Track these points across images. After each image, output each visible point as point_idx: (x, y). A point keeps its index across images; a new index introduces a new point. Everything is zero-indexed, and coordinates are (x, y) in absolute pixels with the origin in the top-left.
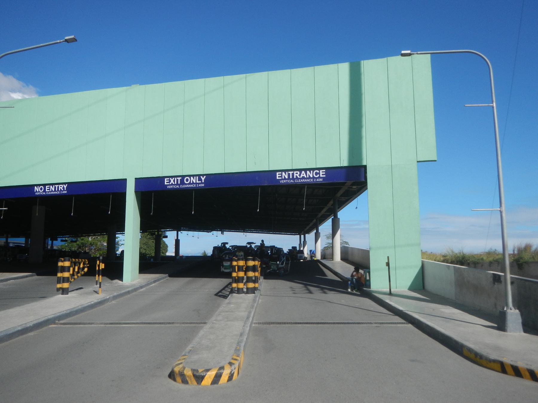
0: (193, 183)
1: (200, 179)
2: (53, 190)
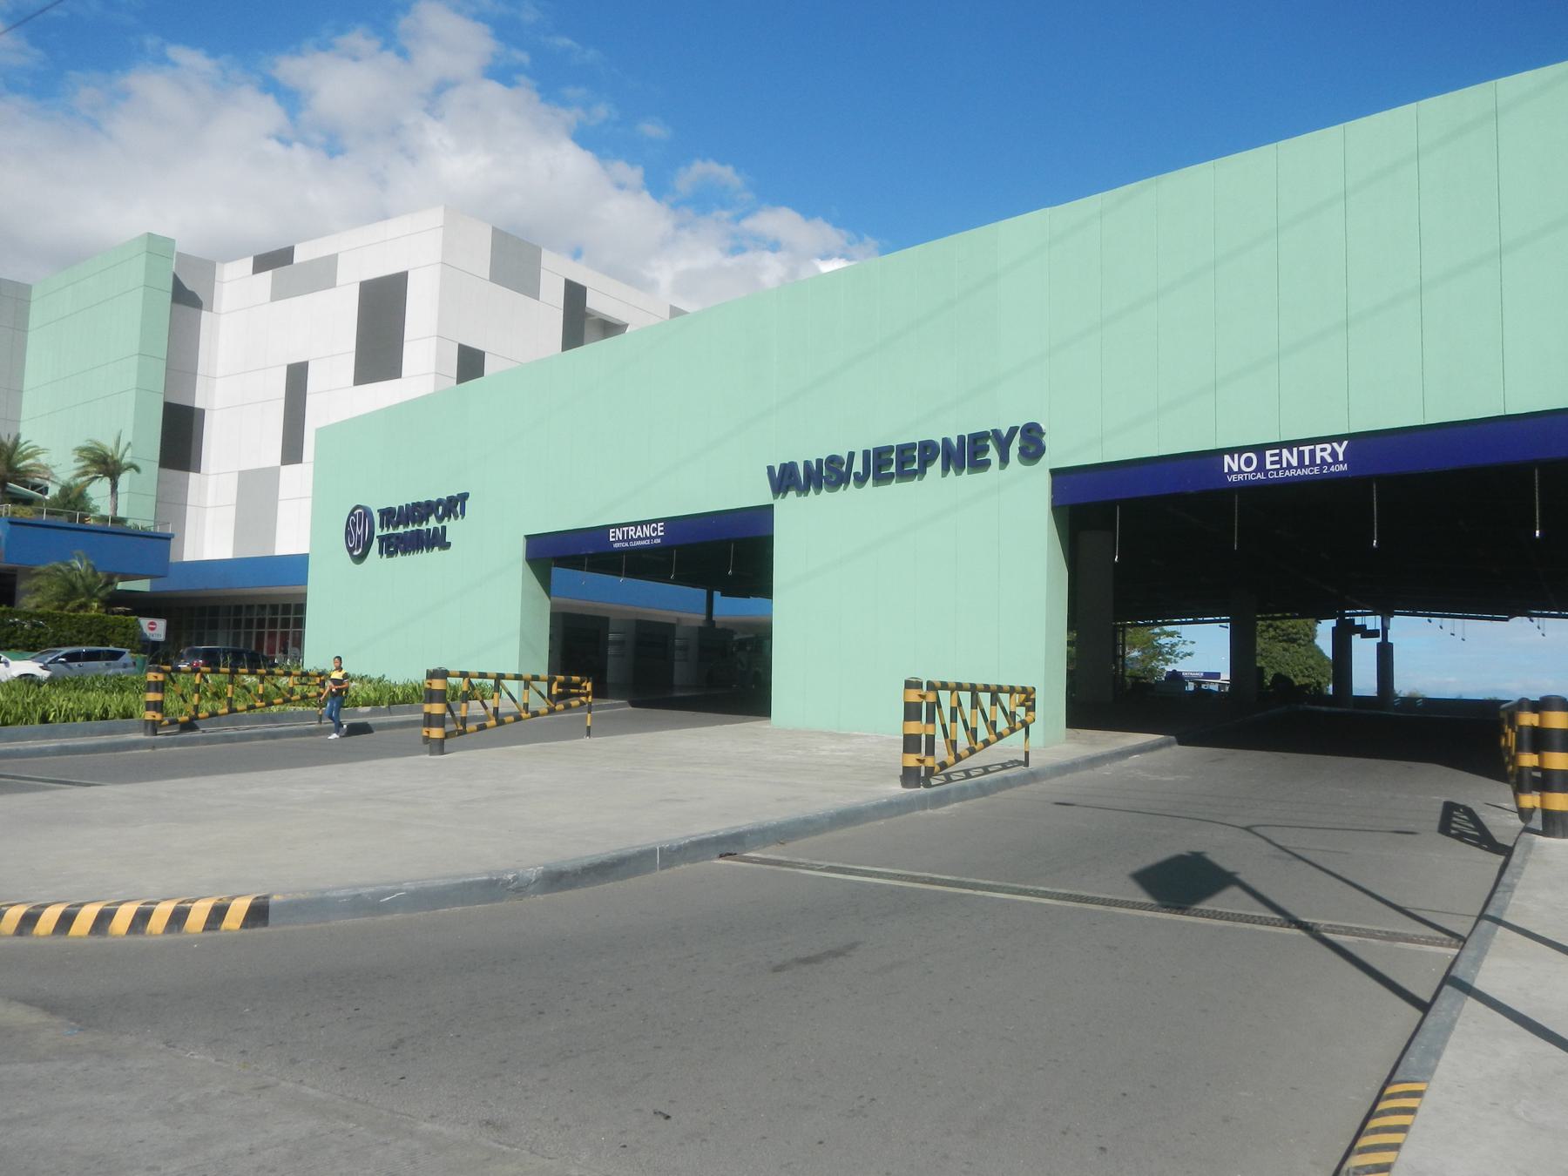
2: (1295, 463)
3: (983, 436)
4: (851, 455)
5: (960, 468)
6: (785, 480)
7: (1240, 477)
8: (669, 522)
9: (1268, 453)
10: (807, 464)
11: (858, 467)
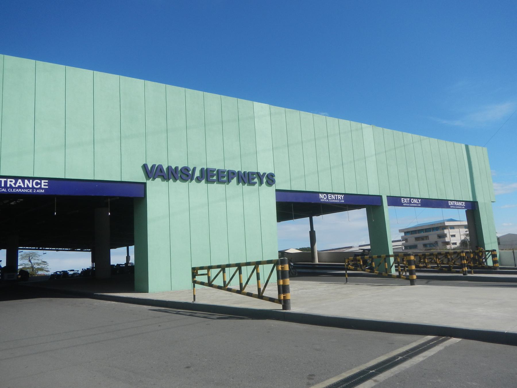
0: (415, 203)
1: (418, 201)
3: (253, 173)
4: (194, 169)
5: (244, 183)
6: (154, 172)
10: (169, 168)
11: (197, 174)
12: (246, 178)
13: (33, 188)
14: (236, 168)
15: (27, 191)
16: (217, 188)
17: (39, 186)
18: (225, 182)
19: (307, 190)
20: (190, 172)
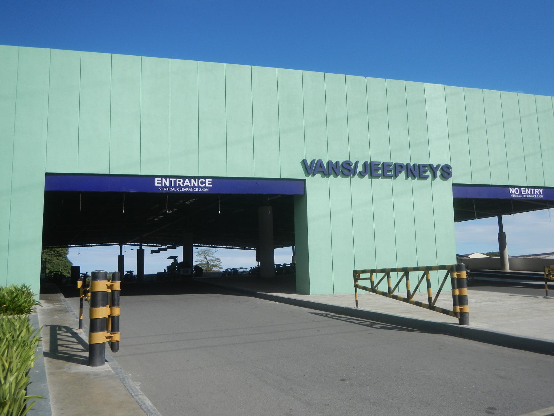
2: (530, 193)
3: (424, 166)
4: (357, 163)
5: (414, 177)
6: (314, 168)
7: (515, 196)
8: (214, 179)
9: (522, 189)
10: (329, 163)
11: (360, 168)
12: (416, 172)
13: (199, 187)
14: (404, 160)
15: (193, 190)
16: (382, 183)
17: (204, 185)
18: (392, 177)
19: (493, 184)
20: (352, 167)
